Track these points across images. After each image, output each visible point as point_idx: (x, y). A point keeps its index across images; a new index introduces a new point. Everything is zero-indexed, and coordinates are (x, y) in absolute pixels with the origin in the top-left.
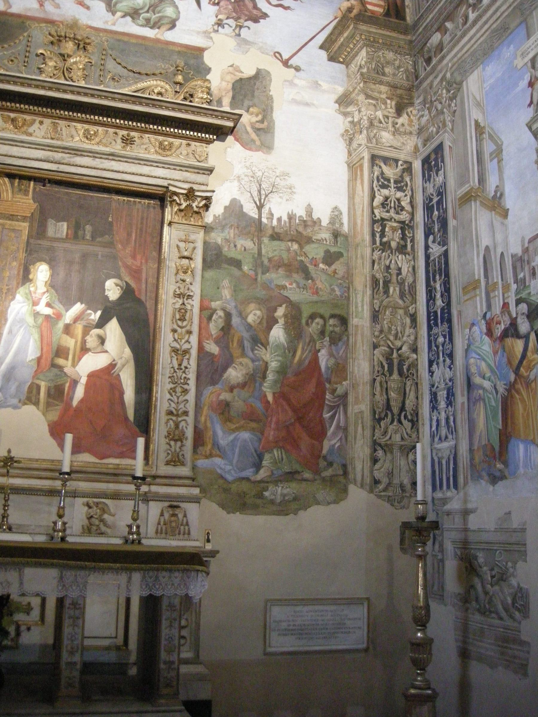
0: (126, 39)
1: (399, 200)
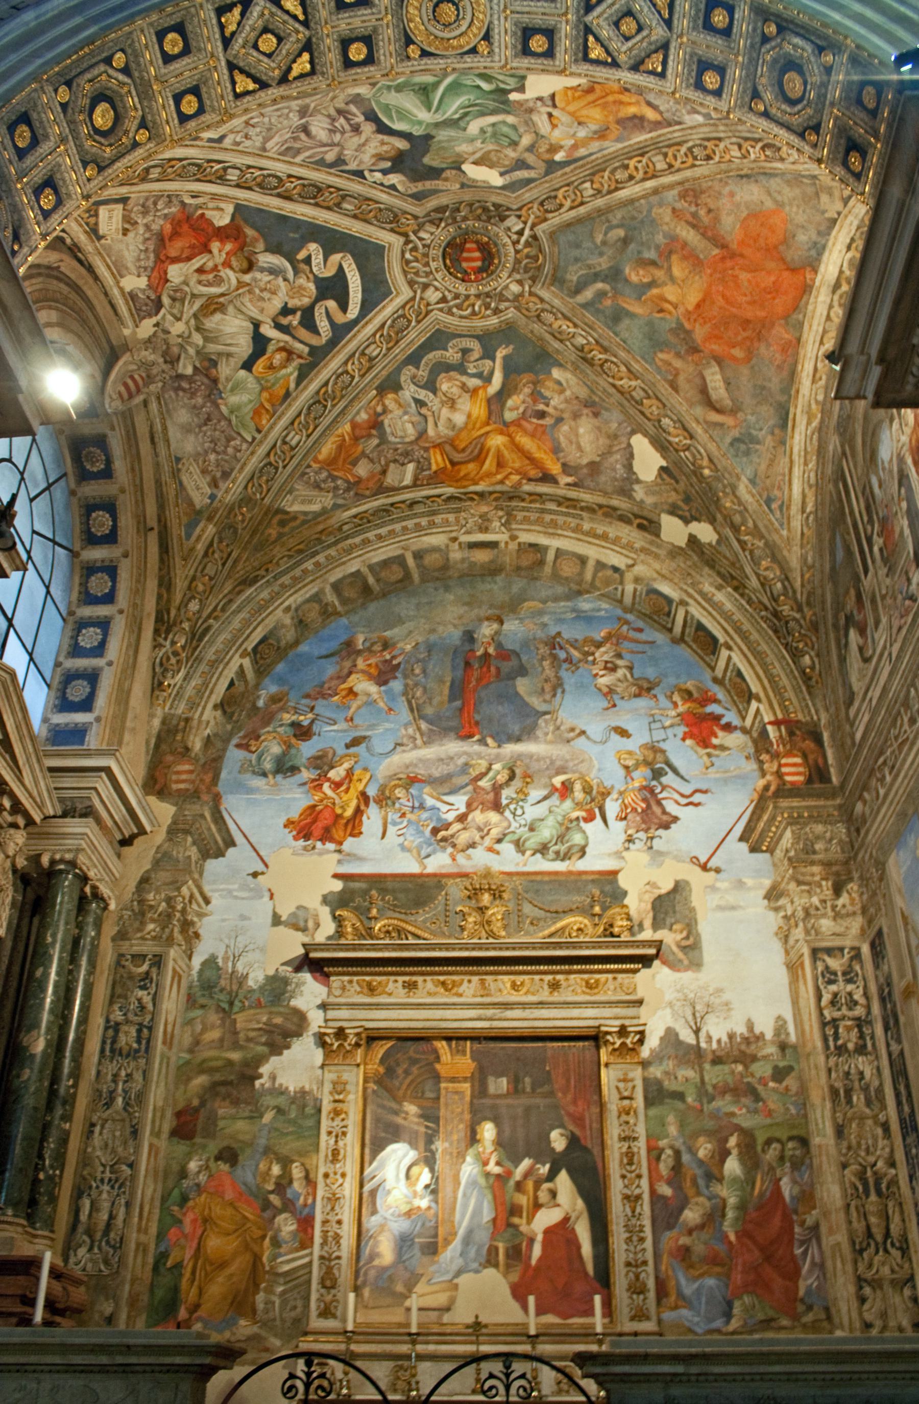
0: (539, 878)
1: (850, 994)
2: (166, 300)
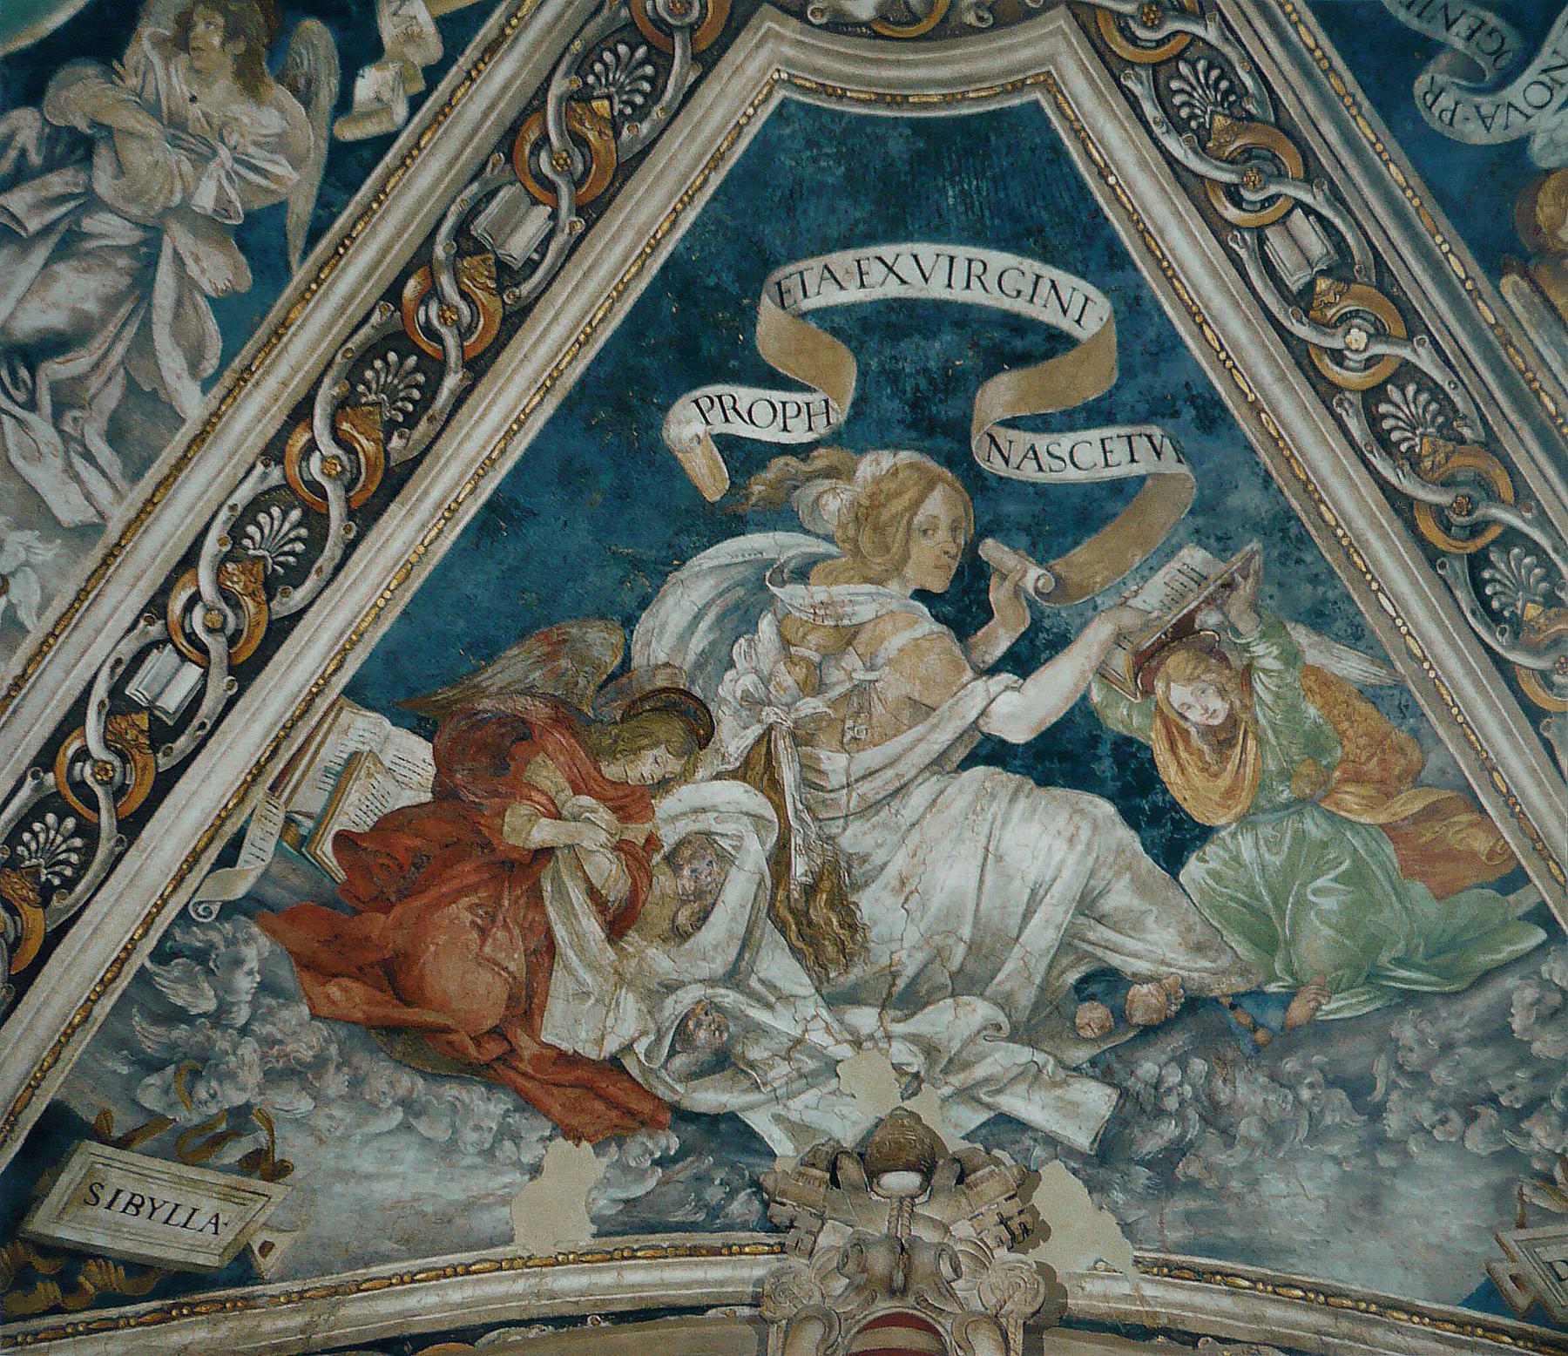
2: (709, 1097)
